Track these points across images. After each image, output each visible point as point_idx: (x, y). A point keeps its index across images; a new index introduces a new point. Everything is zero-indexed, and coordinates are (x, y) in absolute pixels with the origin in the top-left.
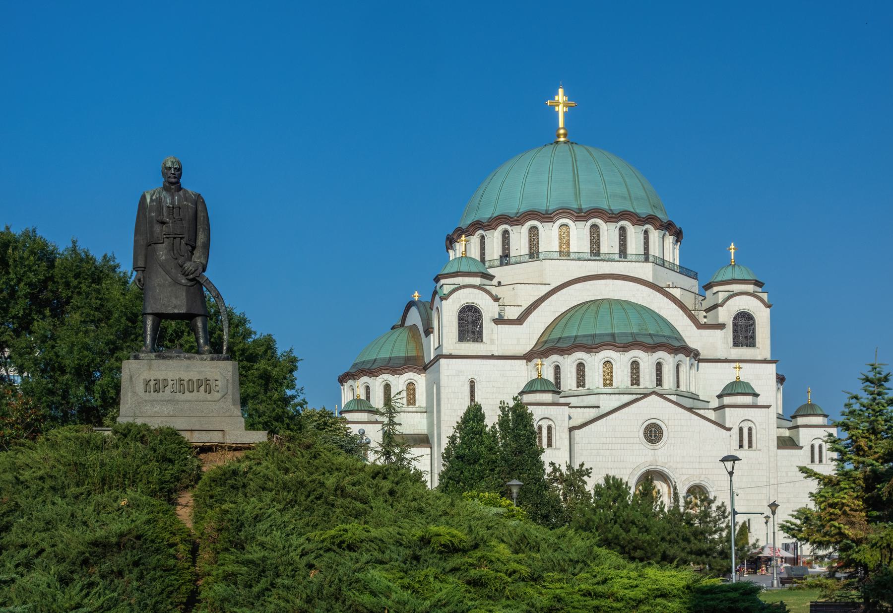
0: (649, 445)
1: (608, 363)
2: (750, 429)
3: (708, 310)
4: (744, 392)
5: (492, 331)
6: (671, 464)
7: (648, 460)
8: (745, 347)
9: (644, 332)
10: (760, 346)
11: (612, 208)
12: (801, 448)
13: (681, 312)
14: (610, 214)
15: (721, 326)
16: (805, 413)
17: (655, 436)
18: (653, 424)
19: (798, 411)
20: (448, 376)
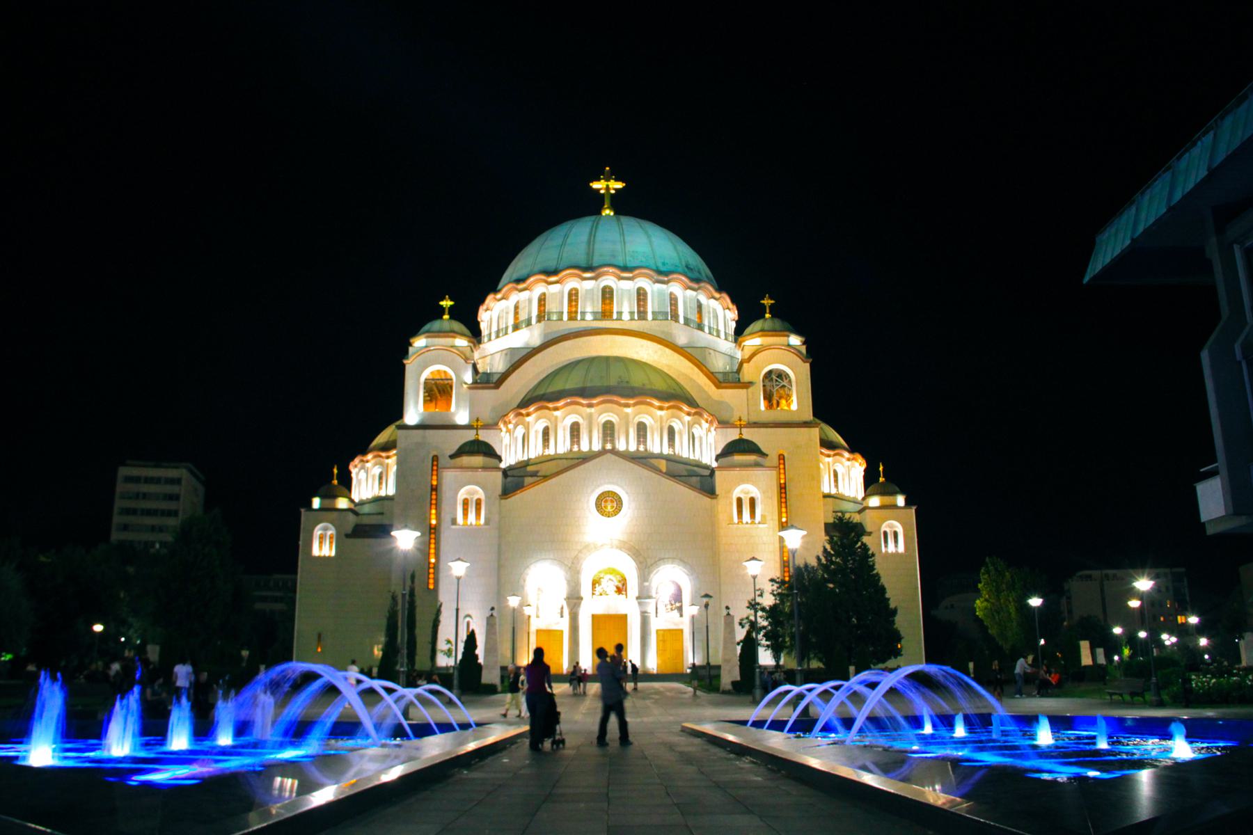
9: (625, 385)
12: (870, 534)
13: (696, 369)
15: (748, 385)
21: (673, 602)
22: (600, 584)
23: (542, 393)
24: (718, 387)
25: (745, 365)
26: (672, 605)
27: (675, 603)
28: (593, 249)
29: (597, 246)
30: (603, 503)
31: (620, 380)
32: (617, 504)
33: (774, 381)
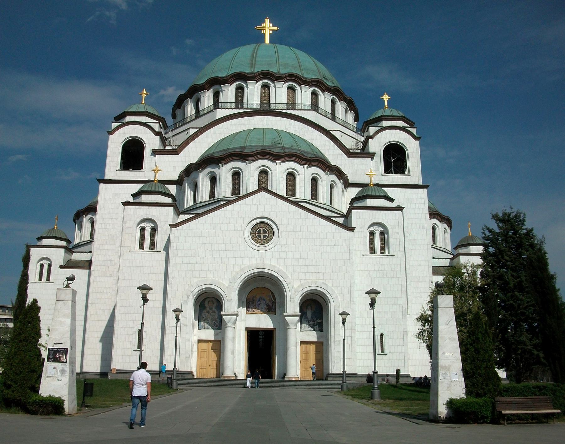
0: (256, 246)
1: (237, 175)
2: (382, 234)
3: (363, 149)
4: (373, 194)
5: (151, 160)
6: (281, 268)
7: (255, 262)
8: (395, 174)
9: (278, 145)
10: (411, 173)
11: (281, 72)
13: (332, 143)
14: (277, 74)
15: (372, 156)
16: (466, 243)
17: (265, 236)
18: (262, 223)
19: (459, 243)
20: (105, 198)
21: (315, 319)
22: (253, 303)
23: (212, 152)
24: (349, 157)
25: (370, 140)
26: (314, 321)
27: (317, 319)
28: (255, 60)
29: (258, 59)
30: (257, 233)
31: (273, 142)
32: (269, 234)
33: (392, 155)
